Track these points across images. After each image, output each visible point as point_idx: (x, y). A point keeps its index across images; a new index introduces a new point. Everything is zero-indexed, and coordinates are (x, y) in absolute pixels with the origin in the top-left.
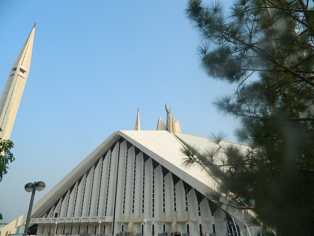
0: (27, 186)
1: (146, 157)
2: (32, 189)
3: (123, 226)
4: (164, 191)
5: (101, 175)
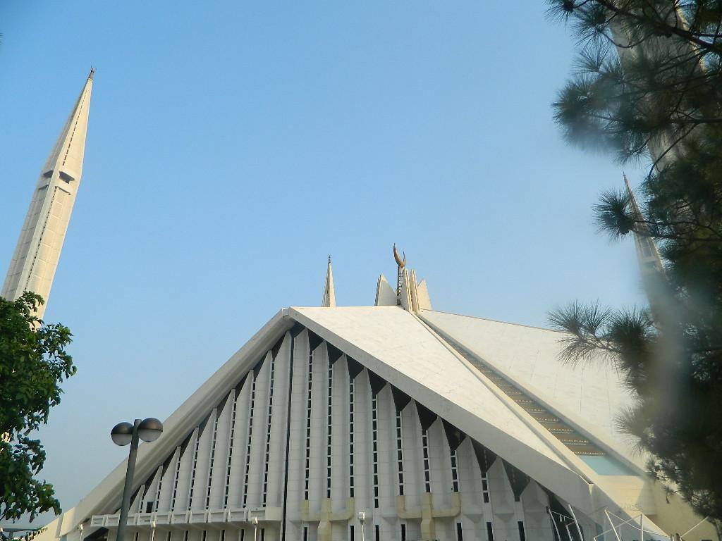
0: (116, 432)
1: (355, 368)
2: (130, 438)
3: (306, 529)
4: (400, 447)
5: (252, 411)
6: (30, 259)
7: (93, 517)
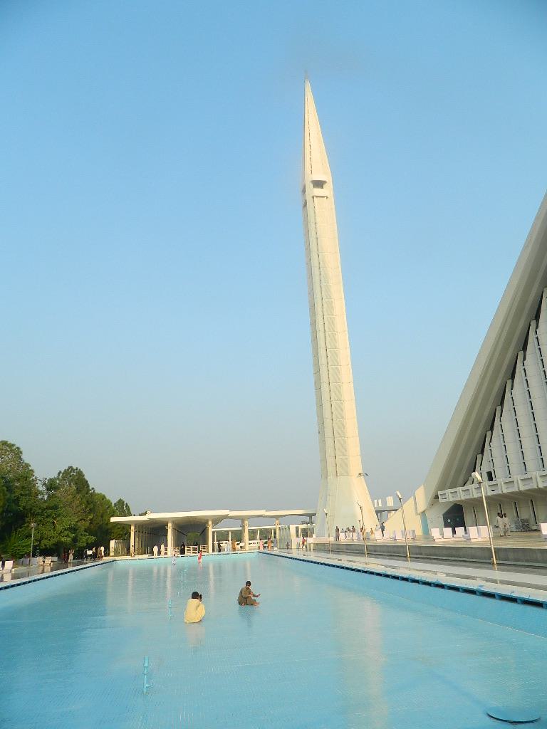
6: (315, 271)
7: (439, 493)
